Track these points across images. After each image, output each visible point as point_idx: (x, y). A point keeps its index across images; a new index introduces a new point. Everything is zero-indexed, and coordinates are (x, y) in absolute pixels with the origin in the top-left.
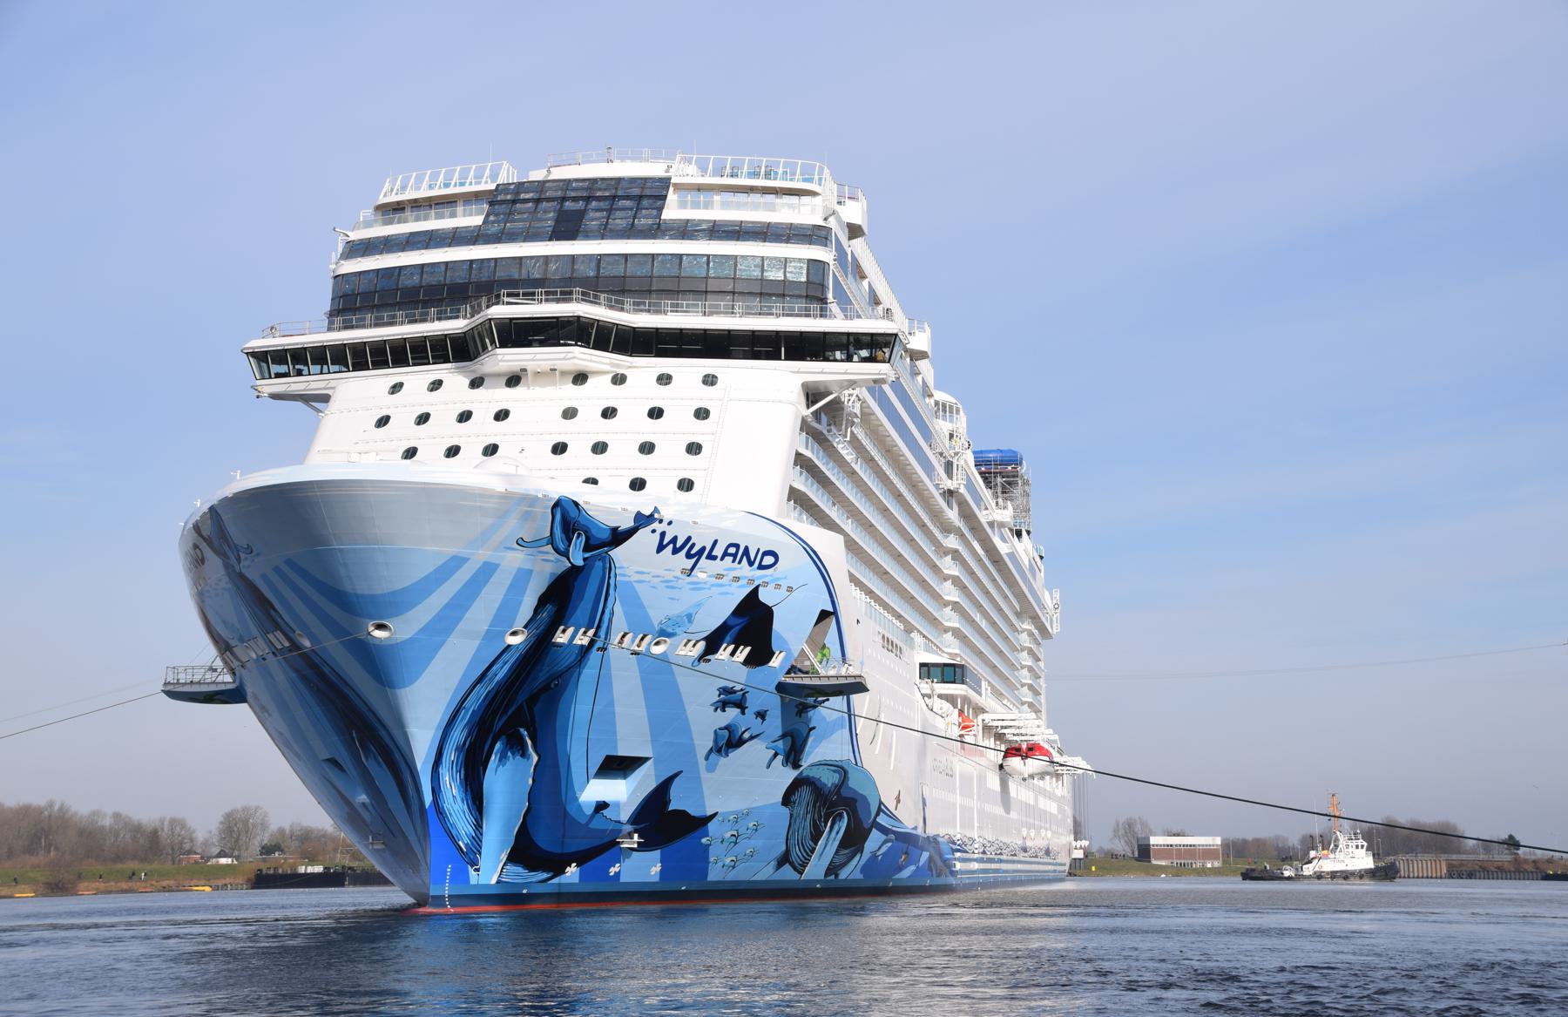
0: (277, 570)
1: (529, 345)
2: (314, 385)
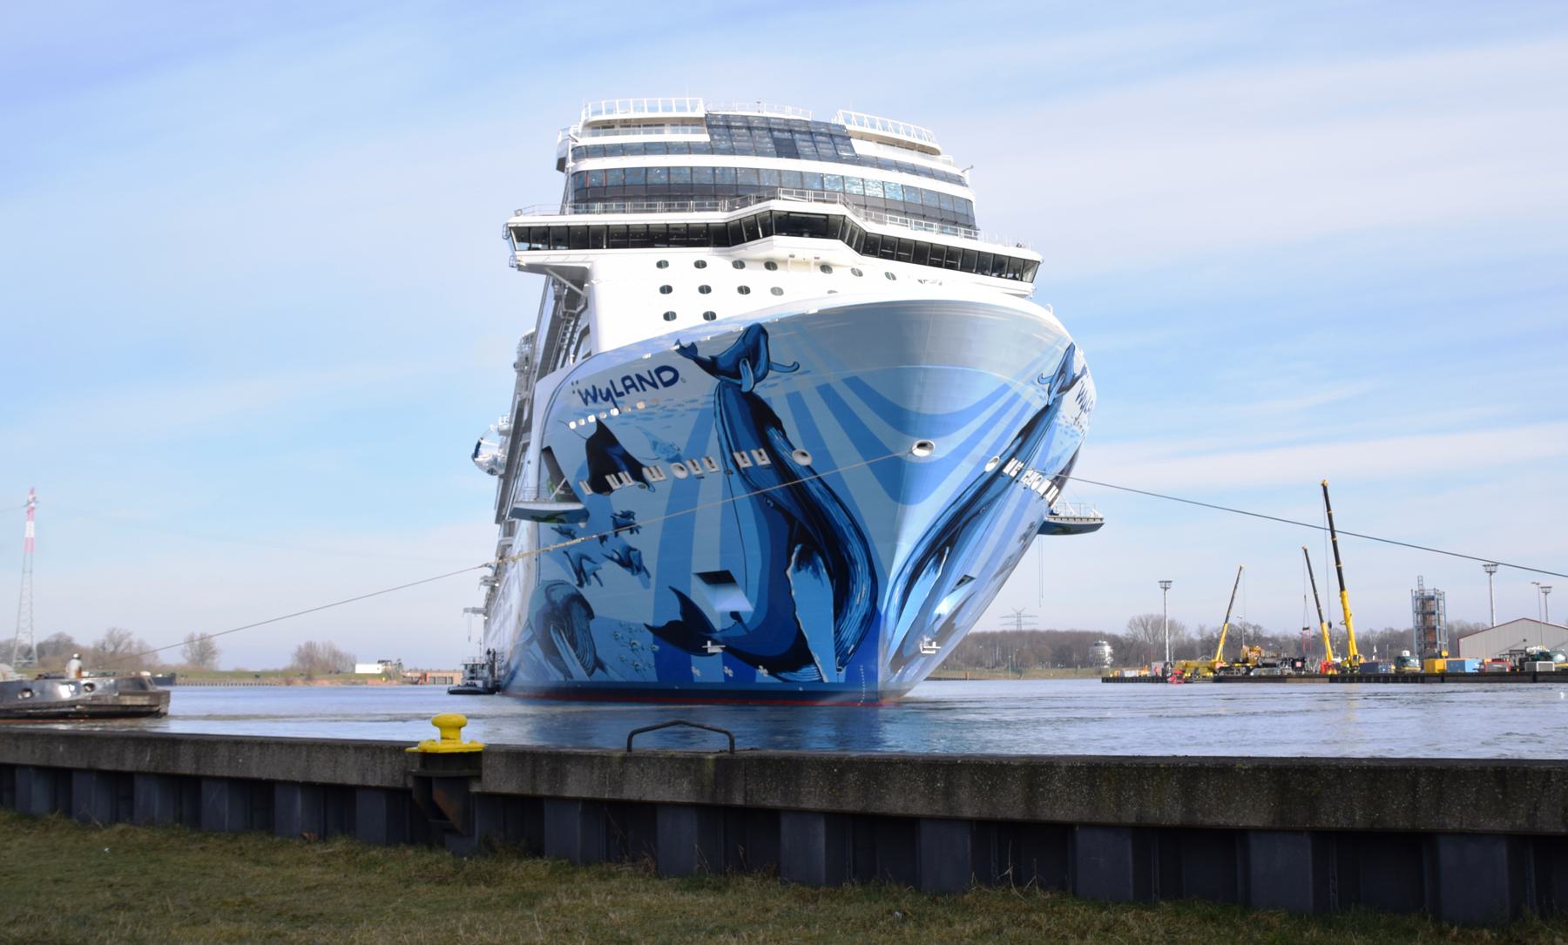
0: (826, 392)
1: (801, 235)
2: (572, 258)
